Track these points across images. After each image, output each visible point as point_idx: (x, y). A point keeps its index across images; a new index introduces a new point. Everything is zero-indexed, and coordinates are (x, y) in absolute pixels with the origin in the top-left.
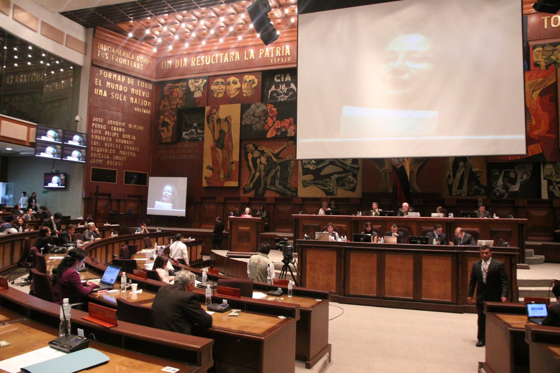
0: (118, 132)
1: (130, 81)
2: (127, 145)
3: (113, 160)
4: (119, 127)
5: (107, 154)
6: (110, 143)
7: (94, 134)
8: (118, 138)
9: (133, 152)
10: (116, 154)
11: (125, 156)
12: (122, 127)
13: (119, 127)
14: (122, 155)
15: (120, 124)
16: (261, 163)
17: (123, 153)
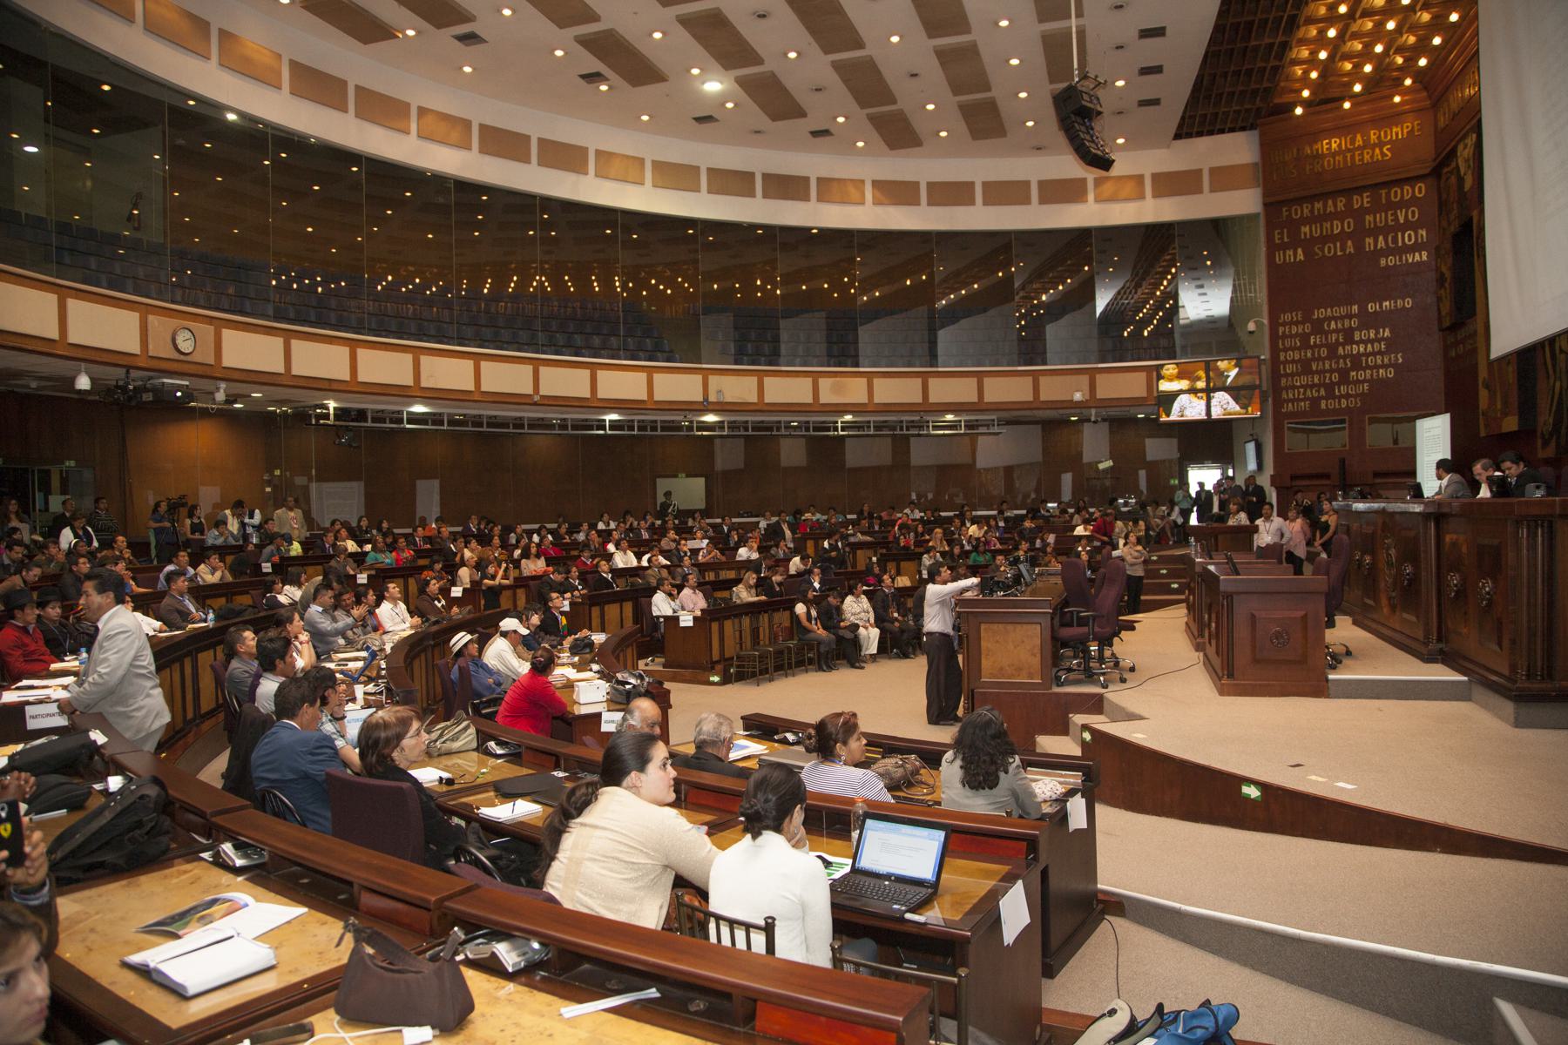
0: (1344, 330)
1: (1365, 200)
2: (1367, 355)
3: (1334, 397)
4: (1342, 318)
5: (1319, 386)
6: (1323, 359)
7: (1286, 350)
8: (1343, 345)
9: (1383, 366)
10: (1339, 384)
11: (1364, 381)
12: (1350, 317)
13: (1342, 318)
14: (1358, 382)
15: (1343, 311)
16: (1561, 351)
17: (1362, 375)
